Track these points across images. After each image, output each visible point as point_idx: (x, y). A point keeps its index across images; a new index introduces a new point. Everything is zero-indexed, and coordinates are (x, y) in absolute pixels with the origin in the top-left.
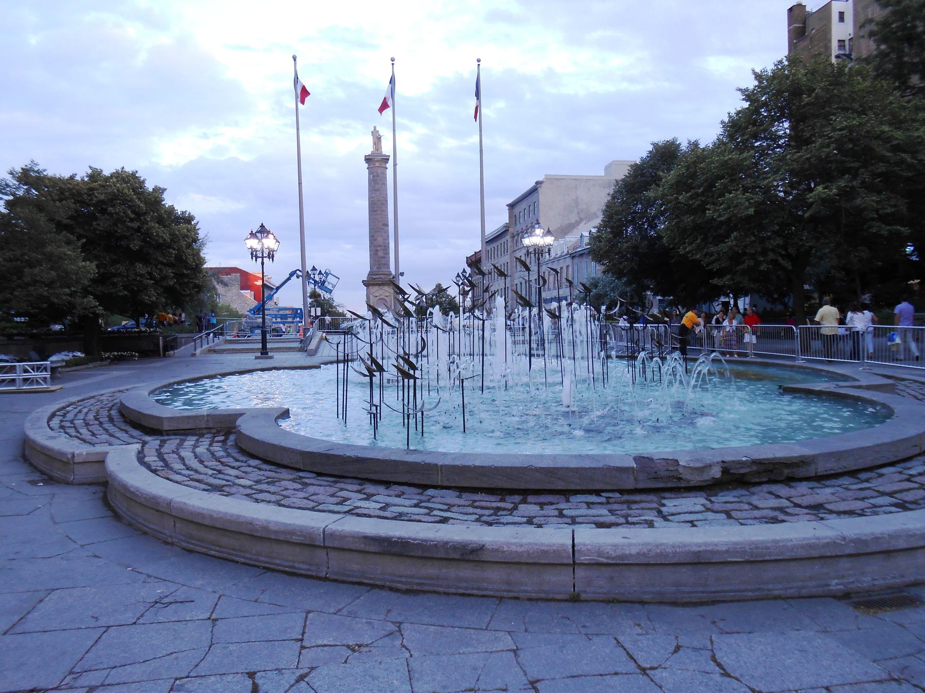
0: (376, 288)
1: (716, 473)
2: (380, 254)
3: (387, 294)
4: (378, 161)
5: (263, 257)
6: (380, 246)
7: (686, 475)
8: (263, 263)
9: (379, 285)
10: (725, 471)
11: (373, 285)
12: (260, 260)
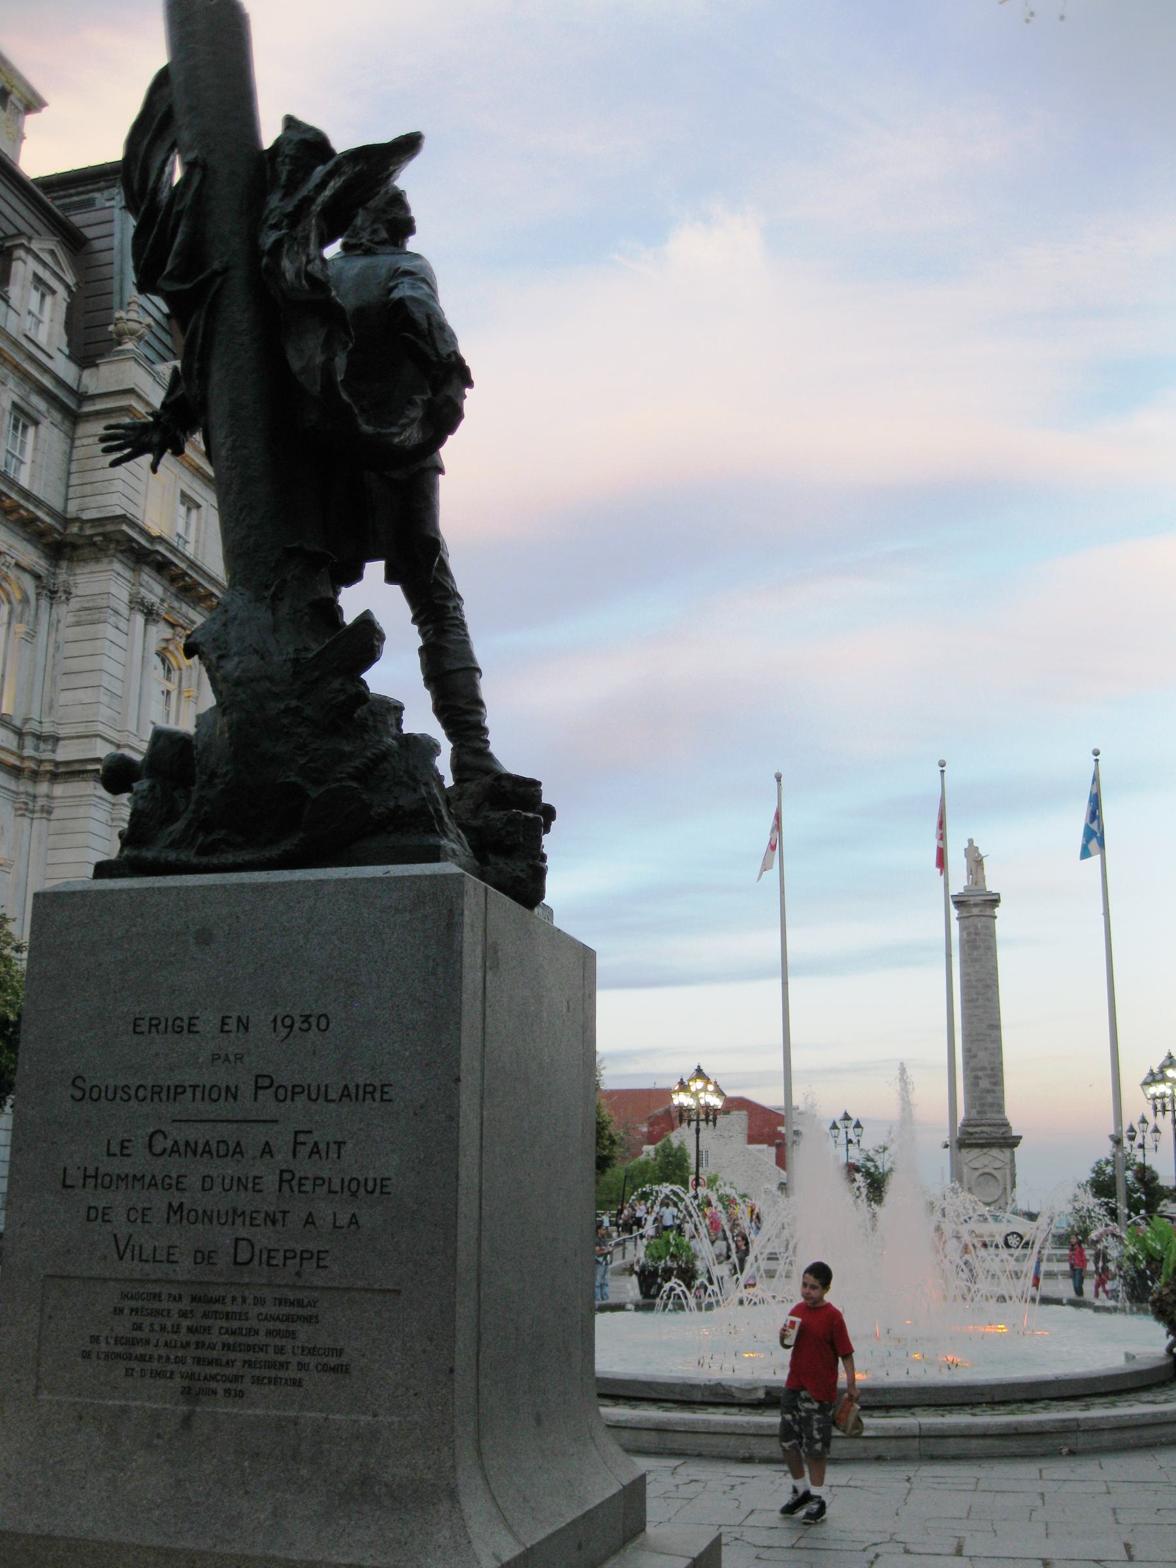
0: (976, 1152)
1: (761, 1394)
2: (985, 1084)
3: (998, 1164)
4: (976, 905)
5: (698, 1121)
6: (983, 1069)
7: (738, 1394)
8: (698, 1131)
9: (981, 1146)
10: (768, 1393)
11: (971, 1146)
12: (694, 1124)
